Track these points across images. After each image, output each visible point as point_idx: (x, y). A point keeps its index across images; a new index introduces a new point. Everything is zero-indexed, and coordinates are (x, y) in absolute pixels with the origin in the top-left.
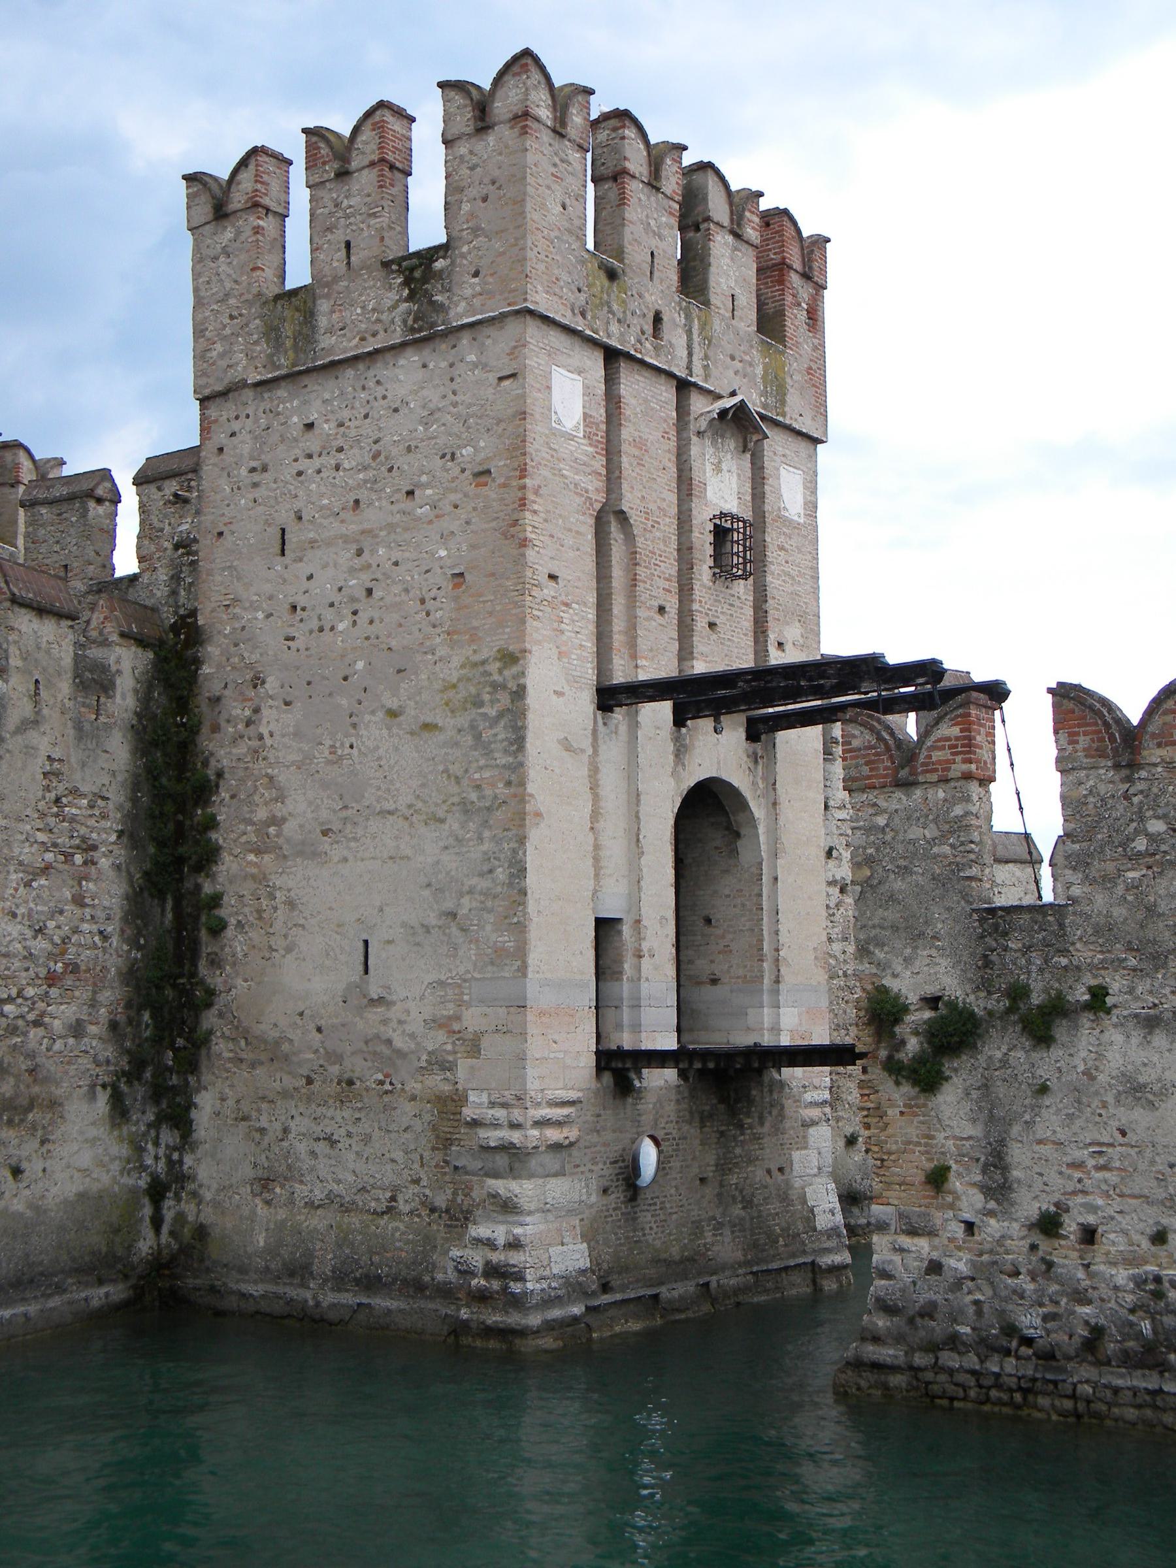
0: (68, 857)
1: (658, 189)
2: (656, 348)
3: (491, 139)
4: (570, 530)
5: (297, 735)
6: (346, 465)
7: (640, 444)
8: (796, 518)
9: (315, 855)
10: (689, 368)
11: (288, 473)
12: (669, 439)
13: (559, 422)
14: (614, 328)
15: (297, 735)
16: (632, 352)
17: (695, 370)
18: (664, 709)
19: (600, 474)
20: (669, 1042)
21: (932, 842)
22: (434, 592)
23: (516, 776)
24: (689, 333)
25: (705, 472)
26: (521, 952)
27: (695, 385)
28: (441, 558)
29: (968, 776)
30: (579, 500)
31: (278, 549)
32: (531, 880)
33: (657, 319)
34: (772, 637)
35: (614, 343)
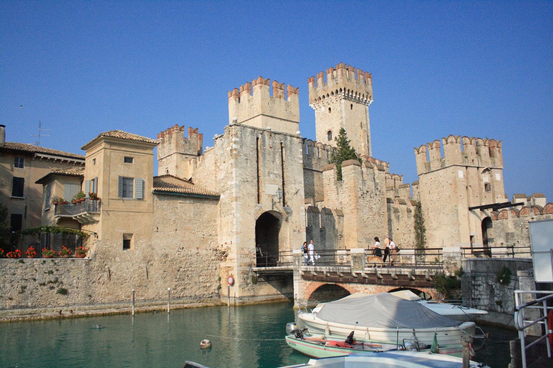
0: (408, 232)
2: (473, 164)
3: (448, 145)
5: (433, 216)
7: (472, 177)
9: (436, 230)
11: (429, 184)
14: (467, 164)
15: (433, 216)
21: (501, 226)
23: (458, 220)
26: (460, 240)
29: (503, 219)
31: (429, 193)
32: (460, 232)
33: (473, 160)
34: (496, 197)
35: (467, 165)
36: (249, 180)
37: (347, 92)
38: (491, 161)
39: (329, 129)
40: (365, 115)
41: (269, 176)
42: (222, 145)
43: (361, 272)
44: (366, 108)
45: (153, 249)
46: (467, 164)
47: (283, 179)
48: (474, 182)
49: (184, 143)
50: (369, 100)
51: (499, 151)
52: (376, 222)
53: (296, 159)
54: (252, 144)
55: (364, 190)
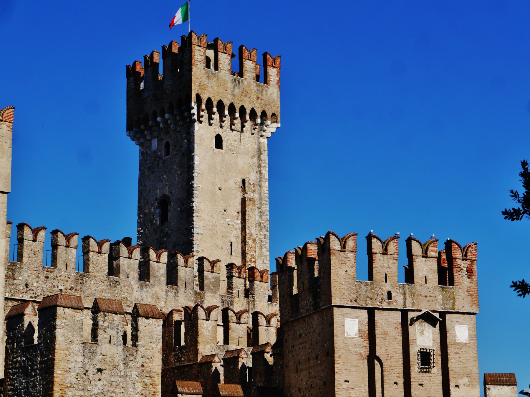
1: (387, 254)
2: (389, 303)
4: (354, 366)
6: (307, 347)
7: (385, 333)
8: (465, 342)
10: (405, 305)
12: (398, 329)
13: (348, 334)
14: (369, 301)
16: (378, 307)
17: (407, 305)
19: (366, 347)
22: (321, 387)
24: (404, 294)
25: (416, 336)
27: (408, 309)
28: (322, 376)
30: (357, 356)
33: (389, 294)
35: (369, 306)
37: (203, 106)
38: (443, 295)
40: (255, 160)
44: (259, 143)
46: (369, 301)
50: (269, 122)
51: (470, 272)
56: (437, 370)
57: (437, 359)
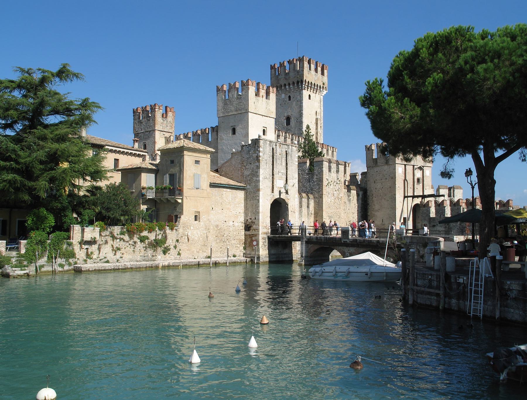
18: (412, 198)
20: (412, 228)
34: (425, 189)
36: (267, 177)
39: (288, 115)
40: (320, 104)
41: (278, 174)
42: (249, 151)
43: (347, 240)
45: (210, 222)
47: (287, 176)
48: (409, 177)
49: (162, 121)
50: (324, 90)
52: (336, 204)
53: (294, 162)
54: (270, 152)
55: (330, 180)
56: (421, 185)
57: (421, 181)
